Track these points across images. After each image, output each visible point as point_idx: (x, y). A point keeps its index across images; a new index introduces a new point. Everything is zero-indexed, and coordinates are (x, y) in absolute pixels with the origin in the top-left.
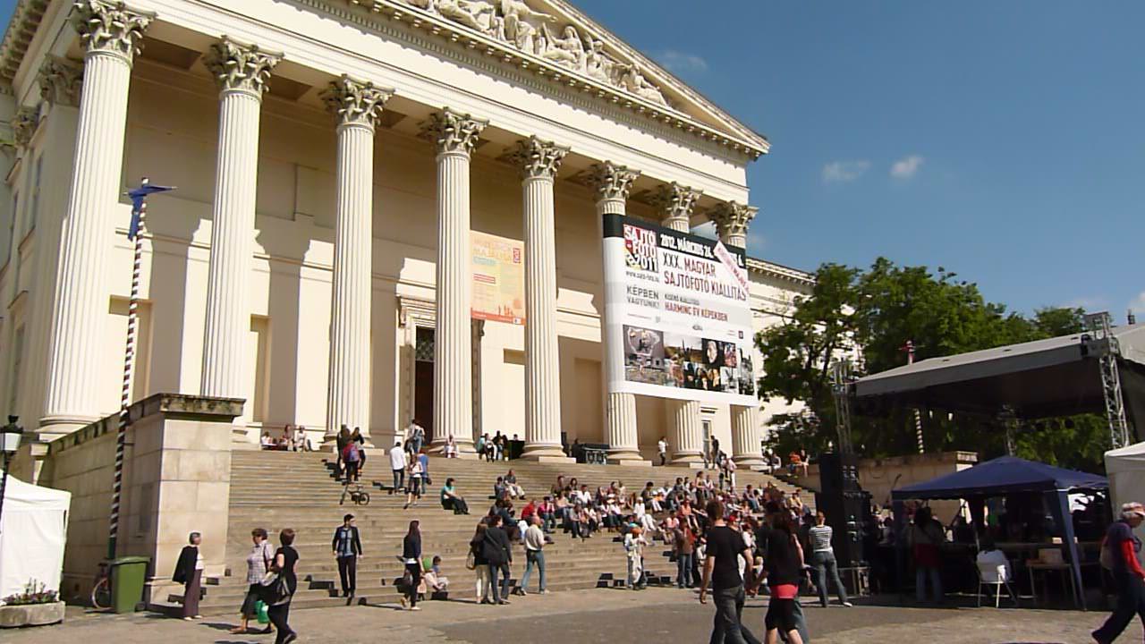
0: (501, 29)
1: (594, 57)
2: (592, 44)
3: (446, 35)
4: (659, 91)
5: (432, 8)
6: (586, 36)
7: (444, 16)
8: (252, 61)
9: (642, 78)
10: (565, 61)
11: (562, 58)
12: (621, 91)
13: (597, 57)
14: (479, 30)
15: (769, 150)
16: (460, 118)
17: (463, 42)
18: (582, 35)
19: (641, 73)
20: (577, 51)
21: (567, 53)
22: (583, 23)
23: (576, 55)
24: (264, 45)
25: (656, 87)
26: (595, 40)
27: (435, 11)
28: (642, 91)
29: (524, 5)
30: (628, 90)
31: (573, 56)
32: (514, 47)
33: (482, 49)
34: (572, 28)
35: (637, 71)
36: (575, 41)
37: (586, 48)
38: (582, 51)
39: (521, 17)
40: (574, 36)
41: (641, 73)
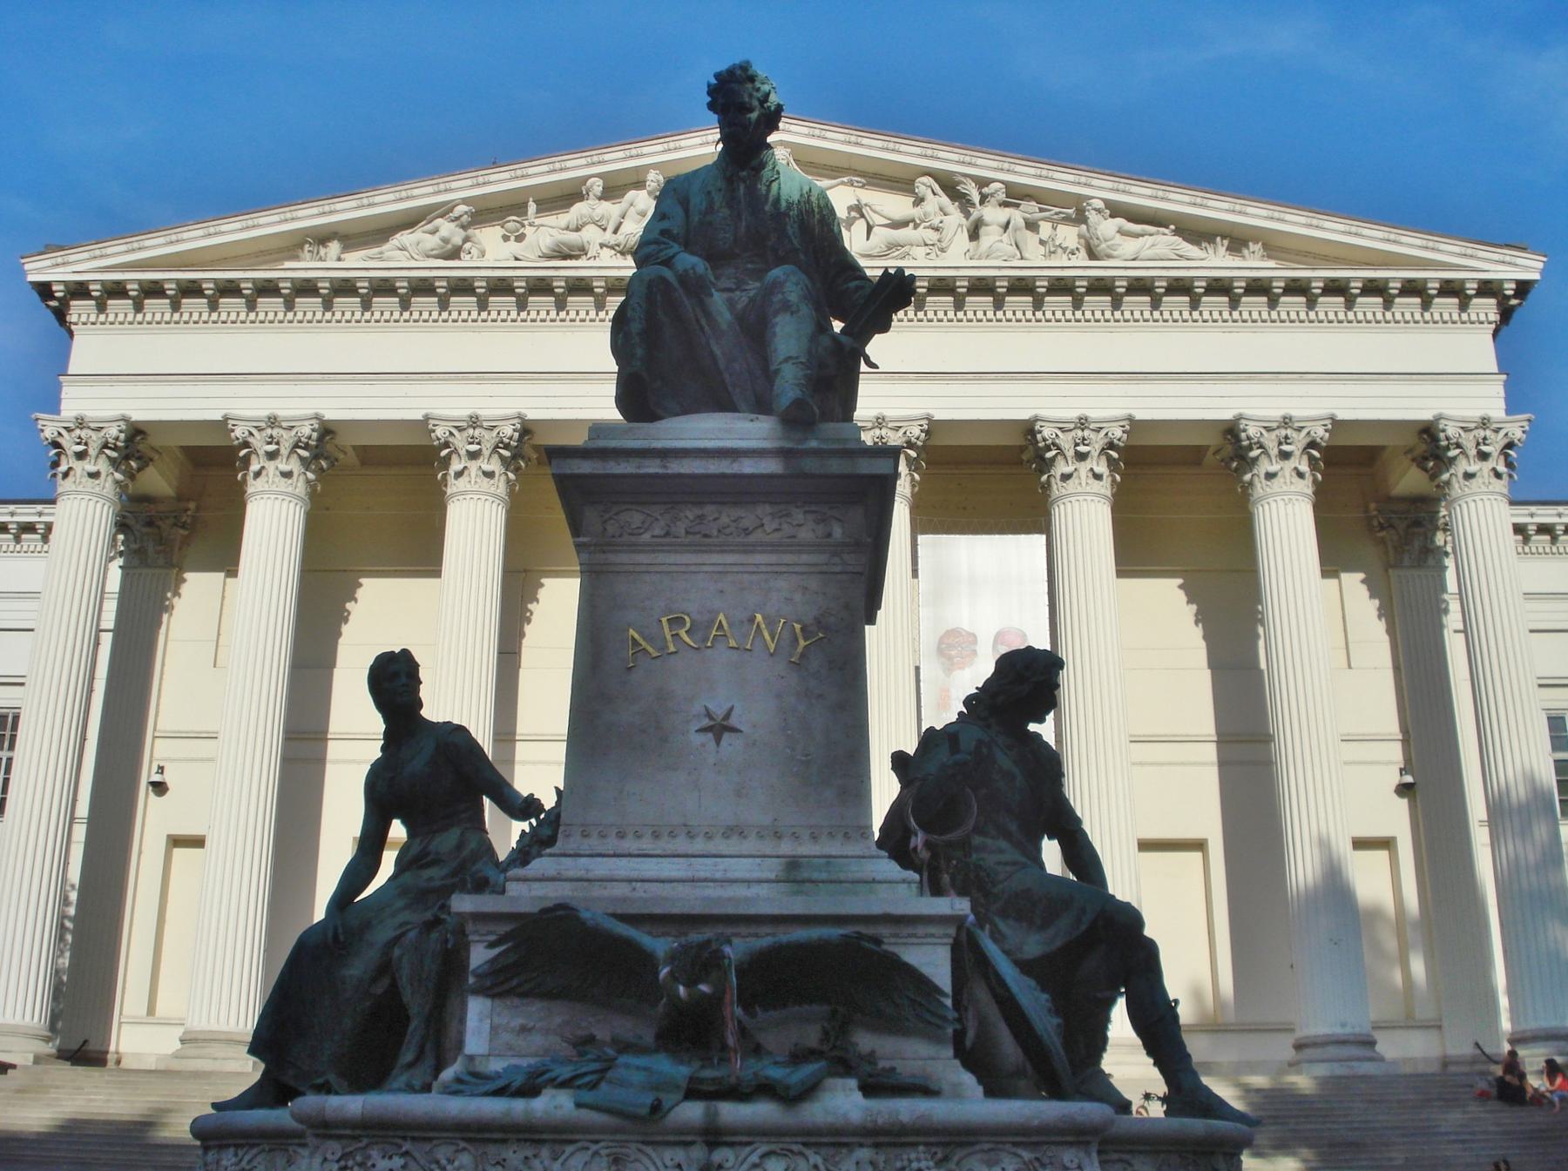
1: (987, 218)
2: (976, 198)
4: (1177, 232)
6: (959, 183)
7: (622, 253)
9: (1120, 221)
10: (906, 249)
11: (893, 246)
13: (993, 214)
15: (1543, 272)
16: (263, 425)
18: (950, 186)
19: (1115, 210)
20: (936, 222)
22: (949, 159)
23: (937, 229)
24: (284, 411)
25: (1167, 227)
26: (982, 183)
27: (606, 252)
28: (1129, 246)
30: (1092, 255)
31: (931, 236)
35: (1099, 211)
38: (955, 218)
40: (934, 194)
41: (1115, 210)
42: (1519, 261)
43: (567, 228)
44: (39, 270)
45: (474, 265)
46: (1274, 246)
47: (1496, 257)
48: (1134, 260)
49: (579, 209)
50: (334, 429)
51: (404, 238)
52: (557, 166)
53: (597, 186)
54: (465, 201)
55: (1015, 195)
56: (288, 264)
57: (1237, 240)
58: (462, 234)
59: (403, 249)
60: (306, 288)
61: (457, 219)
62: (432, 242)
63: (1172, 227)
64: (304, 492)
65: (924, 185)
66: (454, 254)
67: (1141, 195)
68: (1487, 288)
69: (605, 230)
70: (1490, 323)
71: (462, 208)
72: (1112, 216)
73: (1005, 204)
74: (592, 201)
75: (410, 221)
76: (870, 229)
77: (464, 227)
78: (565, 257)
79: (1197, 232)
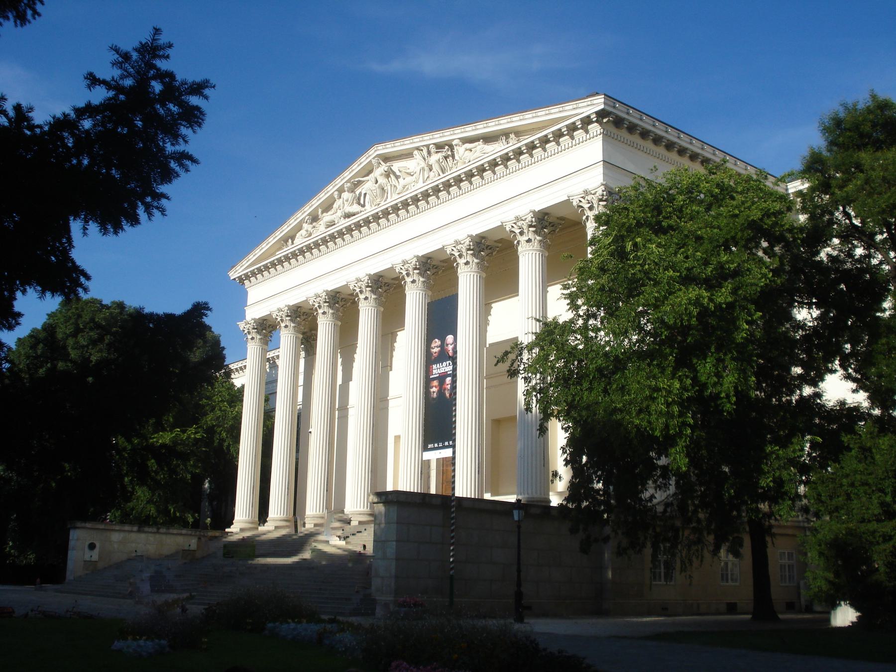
12: (457, 169)
25: (479, 141)
26: (428, 146)
42: (595, 102)
43: (333, 214)
46: (518, 133)
47: (585, 104)
48: (469, 162)
49: (335, 206)
50: (548, 212)
52: (326, 192)
53: (336, 195)
54: (308, 215)
56: (277, 253)
57: (506, 134)
58: (311, 226)
61: (307, 222)
63: (481, 140)
64: (539, 246)
66: (310, 235)
67: (470, 131)
68: (587, 122)
70: (600, 135)
71: (307, 218)
72: (464, 143)
74: (337, 200)
75: (299, 228)
77: (311, 223)
79: (488, 139)
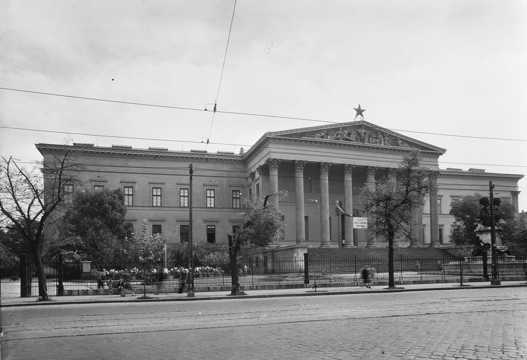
0: (359, 139)
2: (385, 136)
3: (345, 145)
5: (341, 139)
8: (301, 164)
12: (395, 147)
13: (387, 139)
14: (353, 141)
17: (350, 146)
21: (378, 140)
26: (386, 134)
29: (365, 130)
32: (362, 143)
33: (354, 146)
34: (379, 132)
36: (380, 136)
37: (384, 136)
39: (365, 133)
41: (401, 139)
44: (268, 135)
45: (325, 139)
51: (318, 135)
55: (390, 135)
56: (302, 137)
59: (317, 136)
60: (306, 141)
62: (320, 135)
65: (379, 133)
66: (322, 137)
69: (341, 135)
73: (388, 137)
76: (372, 138)
78: (337, 139)
